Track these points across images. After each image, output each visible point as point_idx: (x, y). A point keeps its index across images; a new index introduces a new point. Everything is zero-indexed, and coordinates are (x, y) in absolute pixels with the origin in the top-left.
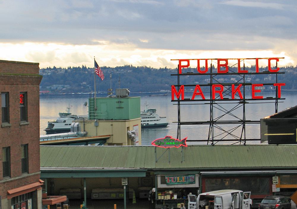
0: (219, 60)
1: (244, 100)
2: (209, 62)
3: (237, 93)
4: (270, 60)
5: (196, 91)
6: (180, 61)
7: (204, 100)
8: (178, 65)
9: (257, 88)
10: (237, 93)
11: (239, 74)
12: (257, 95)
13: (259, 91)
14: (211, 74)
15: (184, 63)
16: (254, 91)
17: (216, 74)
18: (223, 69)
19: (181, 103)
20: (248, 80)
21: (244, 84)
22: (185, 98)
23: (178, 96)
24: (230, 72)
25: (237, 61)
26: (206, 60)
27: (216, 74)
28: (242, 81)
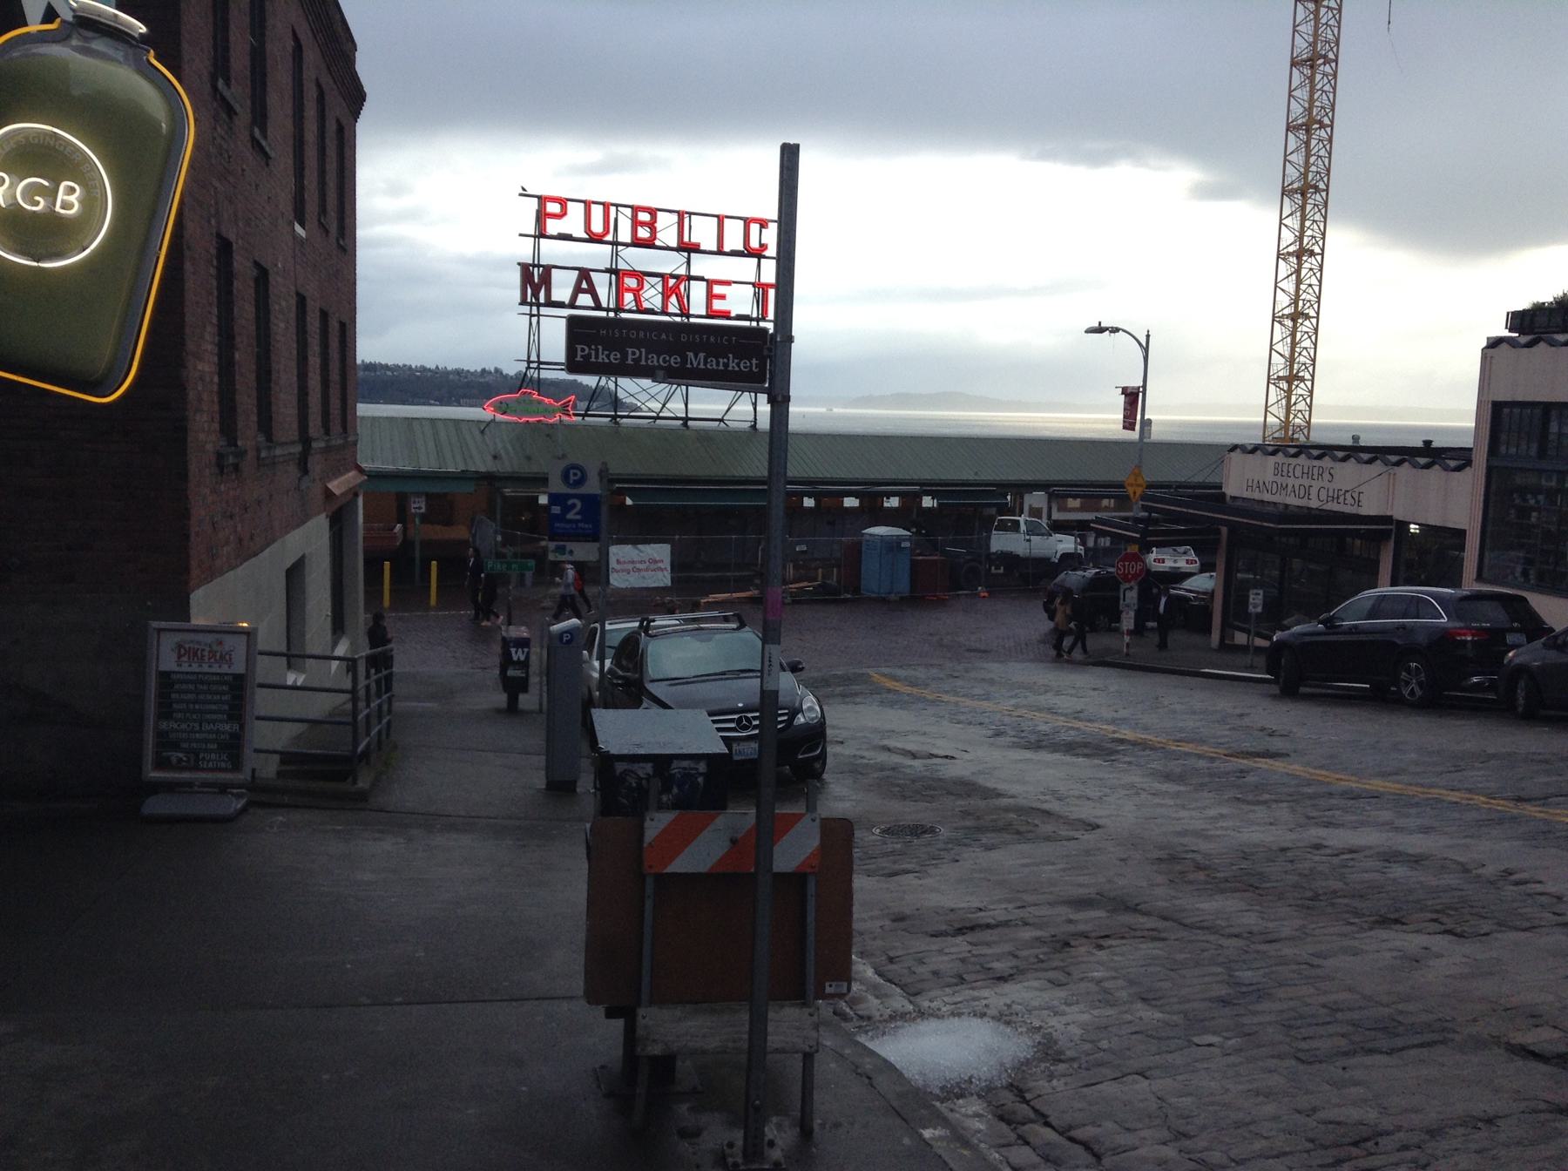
0: (636, 210)
1: (688, 316)
2: (613, 209)
3: (673, 299)
4: (747, 222)
5: (579, 283)
6: (543, 200)
7: (598, 307)
8: (538, 212)
9: (717, 289)
10: (673, 299)
11: (677, 250)
12: (718, 305)
13: (723, 297)
14: (615, 243)
15: (553, 208)
16: (710, 296)
17: (627, 245)
18: (643, 233)
19: (543, 310)
20: (700, 265)
21: (690, 278)
22: (554, 298)
23: (536, 294)
24: (657, 243)
25: (675, 218)
26: (606, 206)
27: (627, 245)
28: (682, 271)
